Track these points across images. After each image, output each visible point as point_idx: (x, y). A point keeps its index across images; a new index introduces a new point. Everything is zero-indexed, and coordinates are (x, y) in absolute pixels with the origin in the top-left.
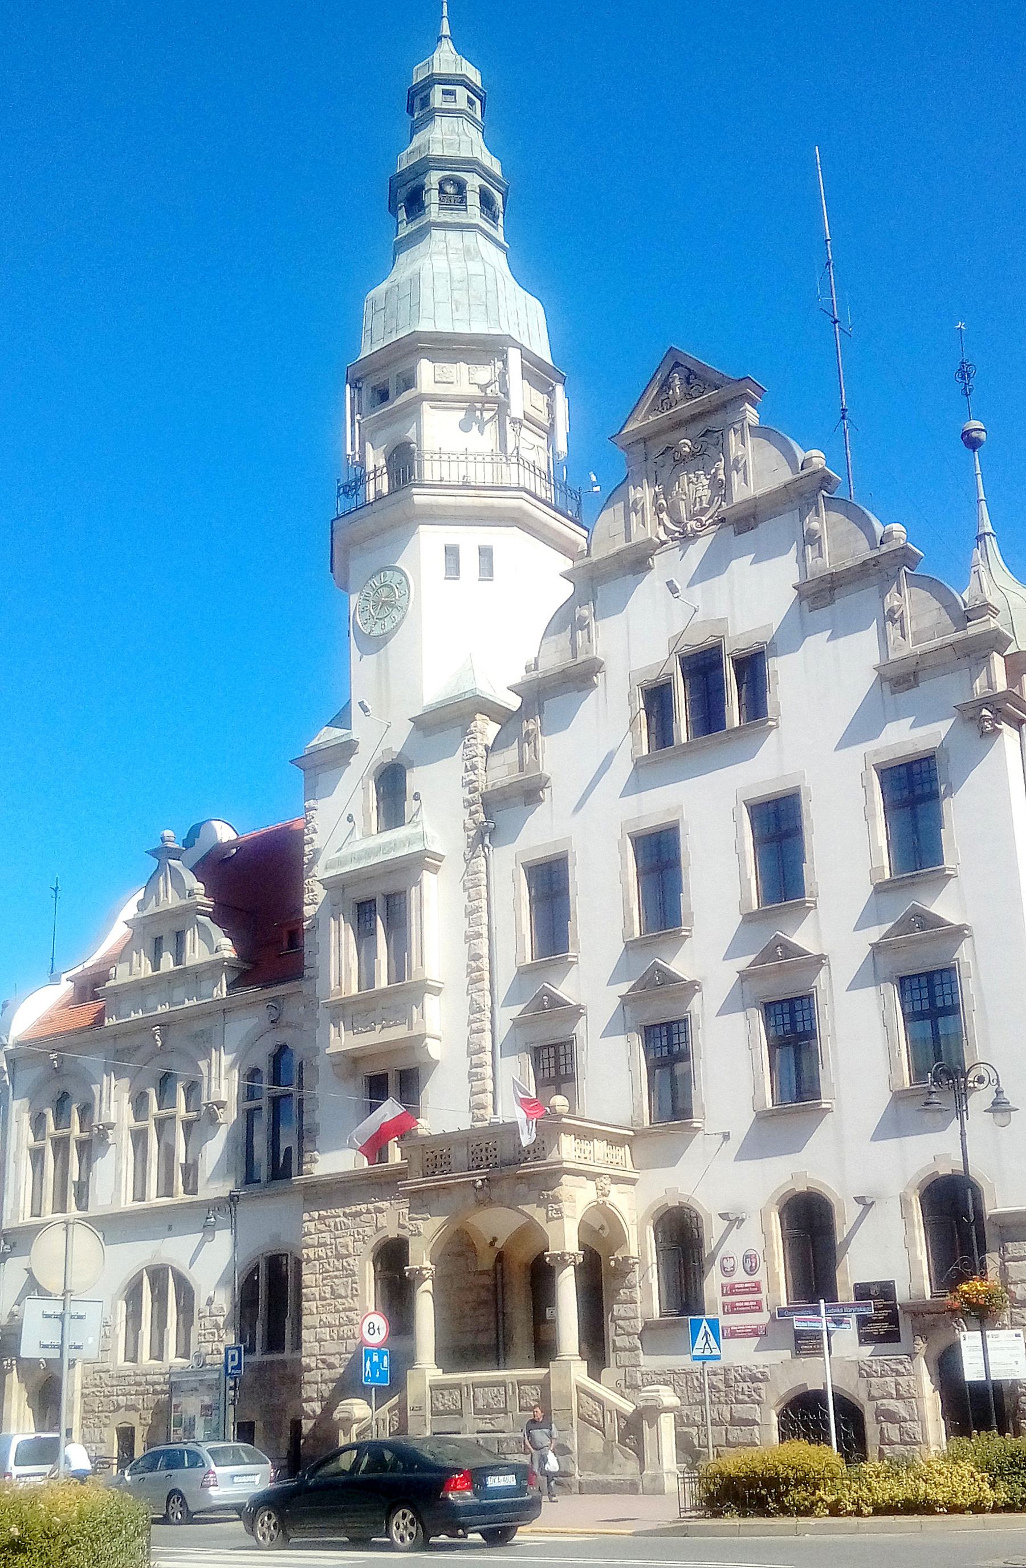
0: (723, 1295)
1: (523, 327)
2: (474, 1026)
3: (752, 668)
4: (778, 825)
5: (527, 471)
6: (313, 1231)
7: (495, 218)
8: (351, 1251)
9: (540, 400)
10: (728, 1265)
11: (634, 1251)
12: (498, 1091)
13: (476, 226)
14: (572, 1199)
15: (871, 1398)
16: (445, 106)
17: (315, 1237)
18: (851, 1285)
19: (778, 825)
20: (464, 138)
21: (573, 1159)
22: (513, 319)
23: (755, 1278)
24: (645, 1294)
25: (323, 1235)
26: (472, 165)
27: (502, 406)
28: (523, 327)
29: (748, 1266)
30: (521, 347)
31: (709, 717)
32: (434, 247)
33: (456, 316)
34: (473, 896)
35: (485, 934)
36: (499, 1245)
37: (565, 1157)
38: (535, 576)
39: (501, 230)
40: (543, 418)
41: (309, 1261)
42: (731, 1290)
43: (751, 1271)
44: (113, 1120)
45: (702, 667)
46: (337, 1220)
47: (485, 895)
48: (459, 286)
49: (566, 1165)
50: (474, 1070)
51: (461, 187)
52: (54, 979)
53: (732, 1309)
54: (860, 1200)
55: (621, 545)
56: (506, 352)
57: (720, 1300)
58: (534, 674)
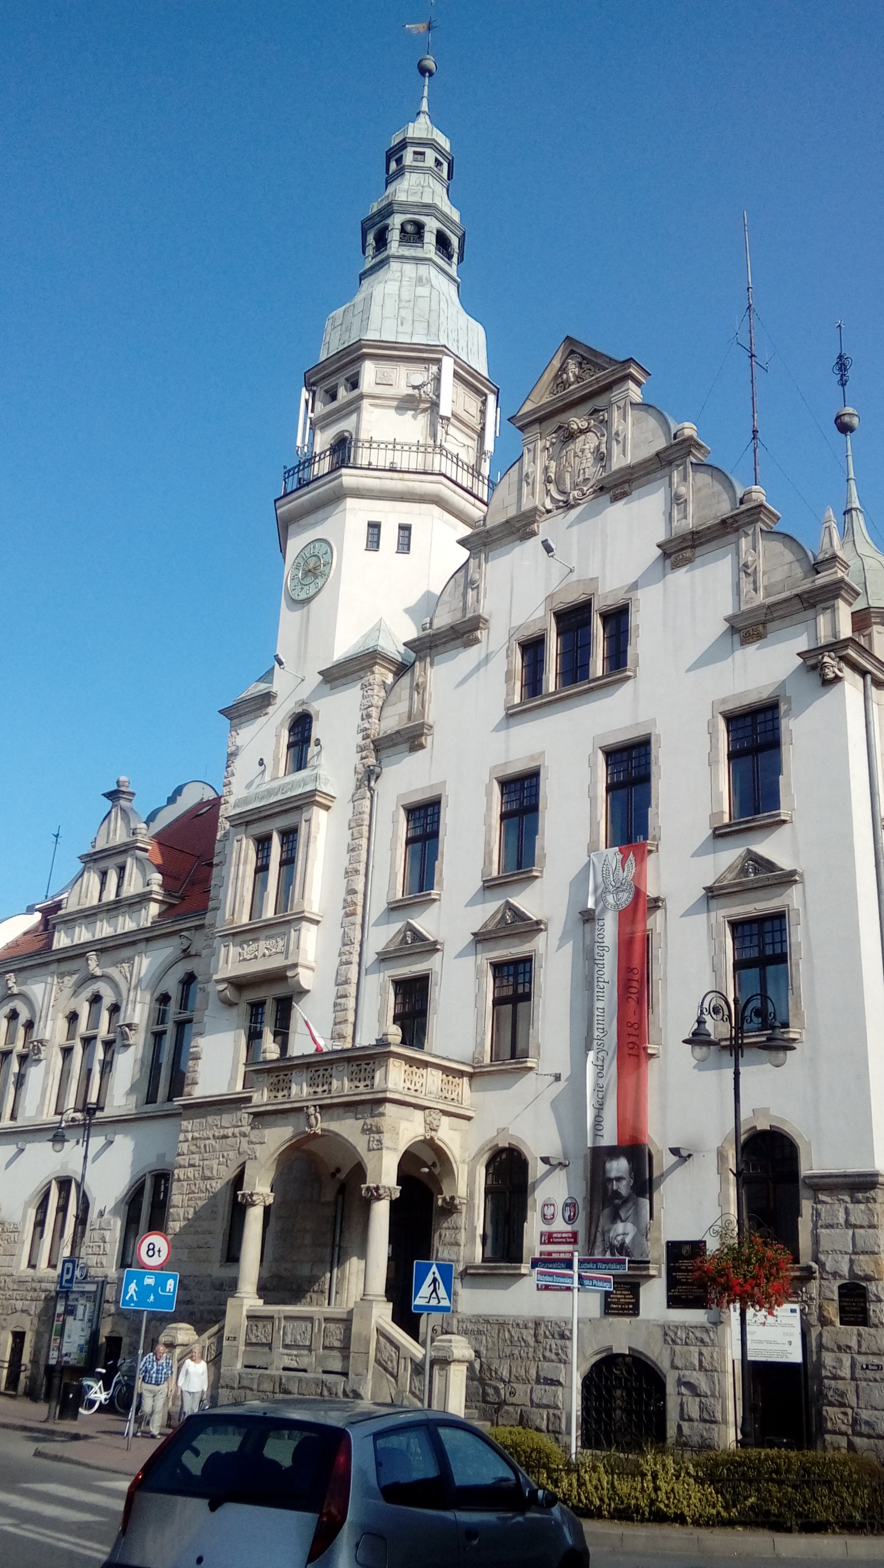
0: (541, 1243)
1: (462, 343)
2: (344, 958)
3: (618, 619)
4: (630, 768)
5: (449, 462)
6: (186, 1152)
7: (450, 257)
8: (215, 1173)
9: (472, 404)
10: (549, 1211)
11: (462, 1190)
12: (359, 1022)
14: (395, 1131)
15: (674, 1367)
17: (186, 1158)
18: (664, 1243)
19: (630, 768)
21: (401, 1089)
22: (453, 335)
24: (466, 1235)
25: (194, 1156)
26: (430, 209)
27: (435, 405)
28: (462, 343)
29: (567, 1215)
30: (456, 358)
31: (575, 669)
32: (390, 275)
33: (400, 329)
34: (356, 835)
35: (363, 871)
36: (342, 1176)
37: (390, 1085)
38: (441, 546)
39: (454, 267)
40: (475, 422)
41: (179, 1180)
42: (549, 1238)
44: (47, 1036)
45: (573, 619)
46: (207, 1142)
47: (366, 834)
48: (406, 305)
49: (389, 1095)
50: (339, 1001)
52: (30, 910)
54: (675, 1151)
55: (512, 512)
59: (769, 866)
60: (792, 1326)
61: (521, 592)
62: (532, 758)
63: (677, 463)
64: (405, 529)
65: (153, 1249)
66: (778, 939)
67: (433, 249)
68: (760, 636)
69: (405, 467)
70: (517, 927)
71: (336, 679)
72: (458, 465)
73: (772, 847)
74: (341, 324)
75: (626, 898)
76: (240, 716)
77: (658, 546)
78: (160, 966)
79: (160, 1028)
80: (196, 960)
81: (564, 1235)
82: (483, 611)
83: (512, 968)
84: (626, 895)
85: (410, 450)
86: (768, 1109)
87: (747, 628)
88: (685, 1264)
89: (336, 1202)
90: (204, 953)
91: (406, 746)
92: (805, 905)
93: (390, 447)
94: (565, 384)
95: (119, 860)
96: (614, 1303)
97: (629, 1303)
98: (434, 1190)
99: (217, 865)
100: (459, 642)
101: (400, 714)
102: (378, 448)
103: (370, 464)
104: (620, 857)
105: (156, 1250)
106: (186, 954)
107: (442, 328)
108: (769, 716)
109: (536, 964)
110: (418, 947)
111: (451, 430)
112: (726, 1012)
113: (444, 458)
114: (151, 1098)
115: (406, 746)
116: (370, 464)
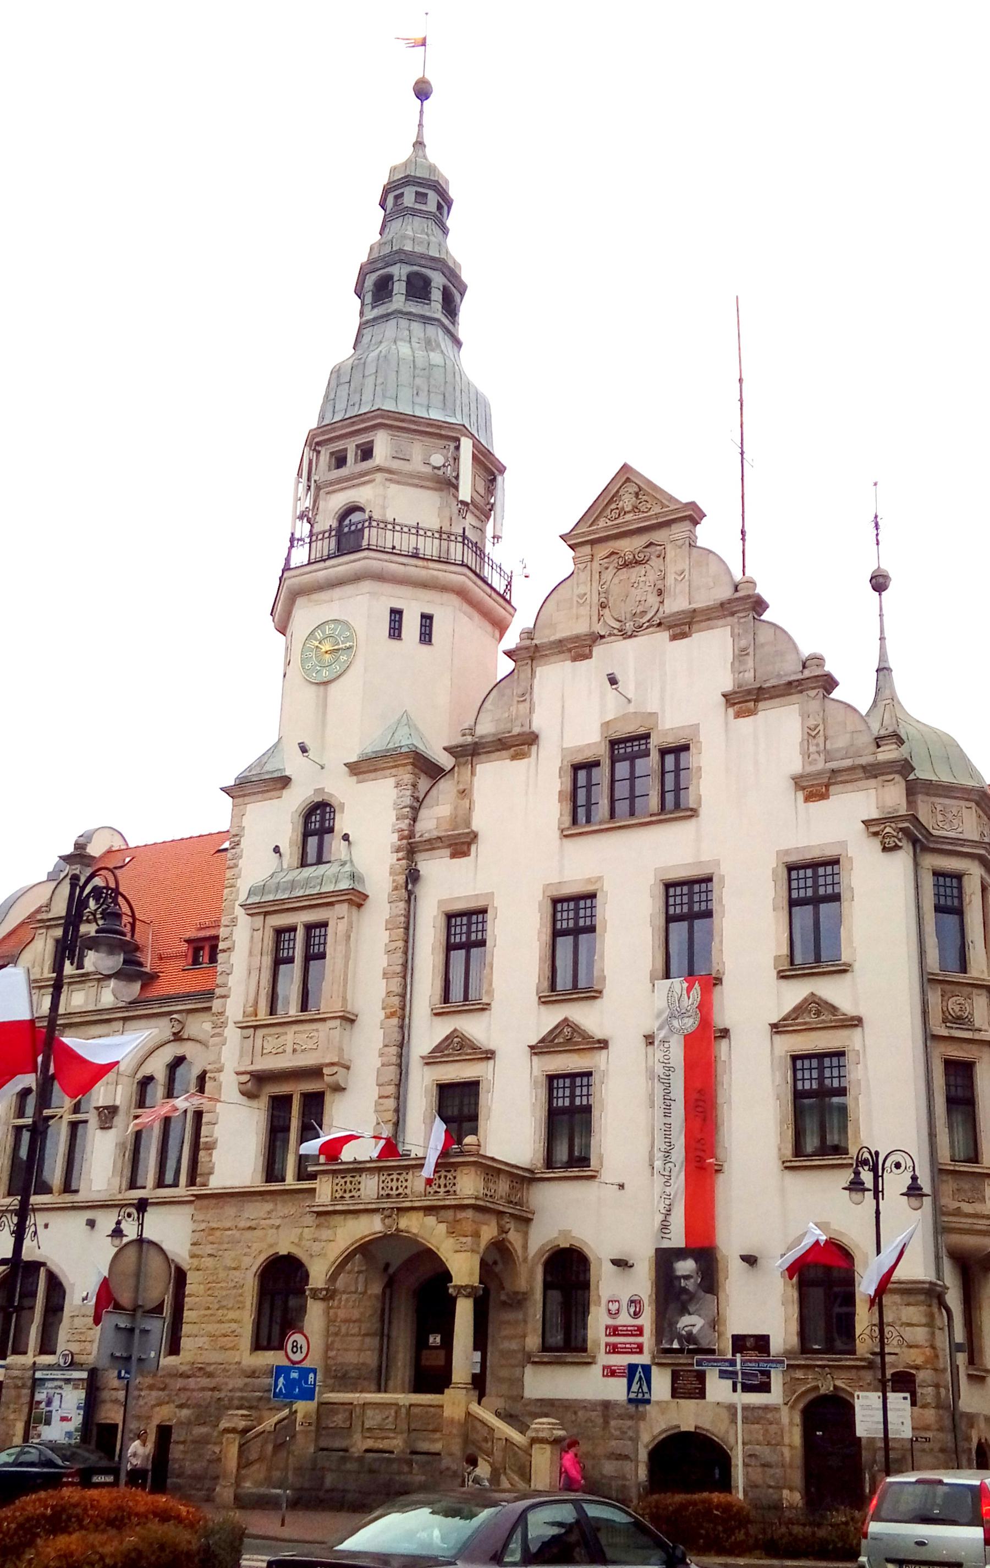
10: (614, 1307)
16: (418, 206)
20: (432, 238)
23: (638, 1322)
29: (632, 1310)
30: (472, 436)
33: (417, 400)
36: (391, 1271)
42: (614, 1331)
43: (636, 1315)
51: (427, 282)
53: (614, 1349)
56: (458, 440)
57: (604, 1340)
58: (469, 739)
59: (833, 1009)
60: (904, 1410)
61: (574, 711)
62: (589, 881)
63: (742, 615)
64: (427, 619)
67: (439, 307)
68: (824, 796)
70: (577, 1043)
75: (690, 1024)
76: (244, 796)
77: (724, 696)
82: (535, 727)
83: (568, 1081)
84: (691, 1020)
87: (814, 788)
89: (384, 1293)
91: (447, 852)
93: (414, 531)
97: (696, 1388)
99: (224, 951)
101: (438, 818)
103: (394, 548)
104: (685, 985)
106: (177, 1037)
107: (458, 402)
109: (595, 1079)
110: (467, 1054)
115: (447, 852)
116: (394, 548)
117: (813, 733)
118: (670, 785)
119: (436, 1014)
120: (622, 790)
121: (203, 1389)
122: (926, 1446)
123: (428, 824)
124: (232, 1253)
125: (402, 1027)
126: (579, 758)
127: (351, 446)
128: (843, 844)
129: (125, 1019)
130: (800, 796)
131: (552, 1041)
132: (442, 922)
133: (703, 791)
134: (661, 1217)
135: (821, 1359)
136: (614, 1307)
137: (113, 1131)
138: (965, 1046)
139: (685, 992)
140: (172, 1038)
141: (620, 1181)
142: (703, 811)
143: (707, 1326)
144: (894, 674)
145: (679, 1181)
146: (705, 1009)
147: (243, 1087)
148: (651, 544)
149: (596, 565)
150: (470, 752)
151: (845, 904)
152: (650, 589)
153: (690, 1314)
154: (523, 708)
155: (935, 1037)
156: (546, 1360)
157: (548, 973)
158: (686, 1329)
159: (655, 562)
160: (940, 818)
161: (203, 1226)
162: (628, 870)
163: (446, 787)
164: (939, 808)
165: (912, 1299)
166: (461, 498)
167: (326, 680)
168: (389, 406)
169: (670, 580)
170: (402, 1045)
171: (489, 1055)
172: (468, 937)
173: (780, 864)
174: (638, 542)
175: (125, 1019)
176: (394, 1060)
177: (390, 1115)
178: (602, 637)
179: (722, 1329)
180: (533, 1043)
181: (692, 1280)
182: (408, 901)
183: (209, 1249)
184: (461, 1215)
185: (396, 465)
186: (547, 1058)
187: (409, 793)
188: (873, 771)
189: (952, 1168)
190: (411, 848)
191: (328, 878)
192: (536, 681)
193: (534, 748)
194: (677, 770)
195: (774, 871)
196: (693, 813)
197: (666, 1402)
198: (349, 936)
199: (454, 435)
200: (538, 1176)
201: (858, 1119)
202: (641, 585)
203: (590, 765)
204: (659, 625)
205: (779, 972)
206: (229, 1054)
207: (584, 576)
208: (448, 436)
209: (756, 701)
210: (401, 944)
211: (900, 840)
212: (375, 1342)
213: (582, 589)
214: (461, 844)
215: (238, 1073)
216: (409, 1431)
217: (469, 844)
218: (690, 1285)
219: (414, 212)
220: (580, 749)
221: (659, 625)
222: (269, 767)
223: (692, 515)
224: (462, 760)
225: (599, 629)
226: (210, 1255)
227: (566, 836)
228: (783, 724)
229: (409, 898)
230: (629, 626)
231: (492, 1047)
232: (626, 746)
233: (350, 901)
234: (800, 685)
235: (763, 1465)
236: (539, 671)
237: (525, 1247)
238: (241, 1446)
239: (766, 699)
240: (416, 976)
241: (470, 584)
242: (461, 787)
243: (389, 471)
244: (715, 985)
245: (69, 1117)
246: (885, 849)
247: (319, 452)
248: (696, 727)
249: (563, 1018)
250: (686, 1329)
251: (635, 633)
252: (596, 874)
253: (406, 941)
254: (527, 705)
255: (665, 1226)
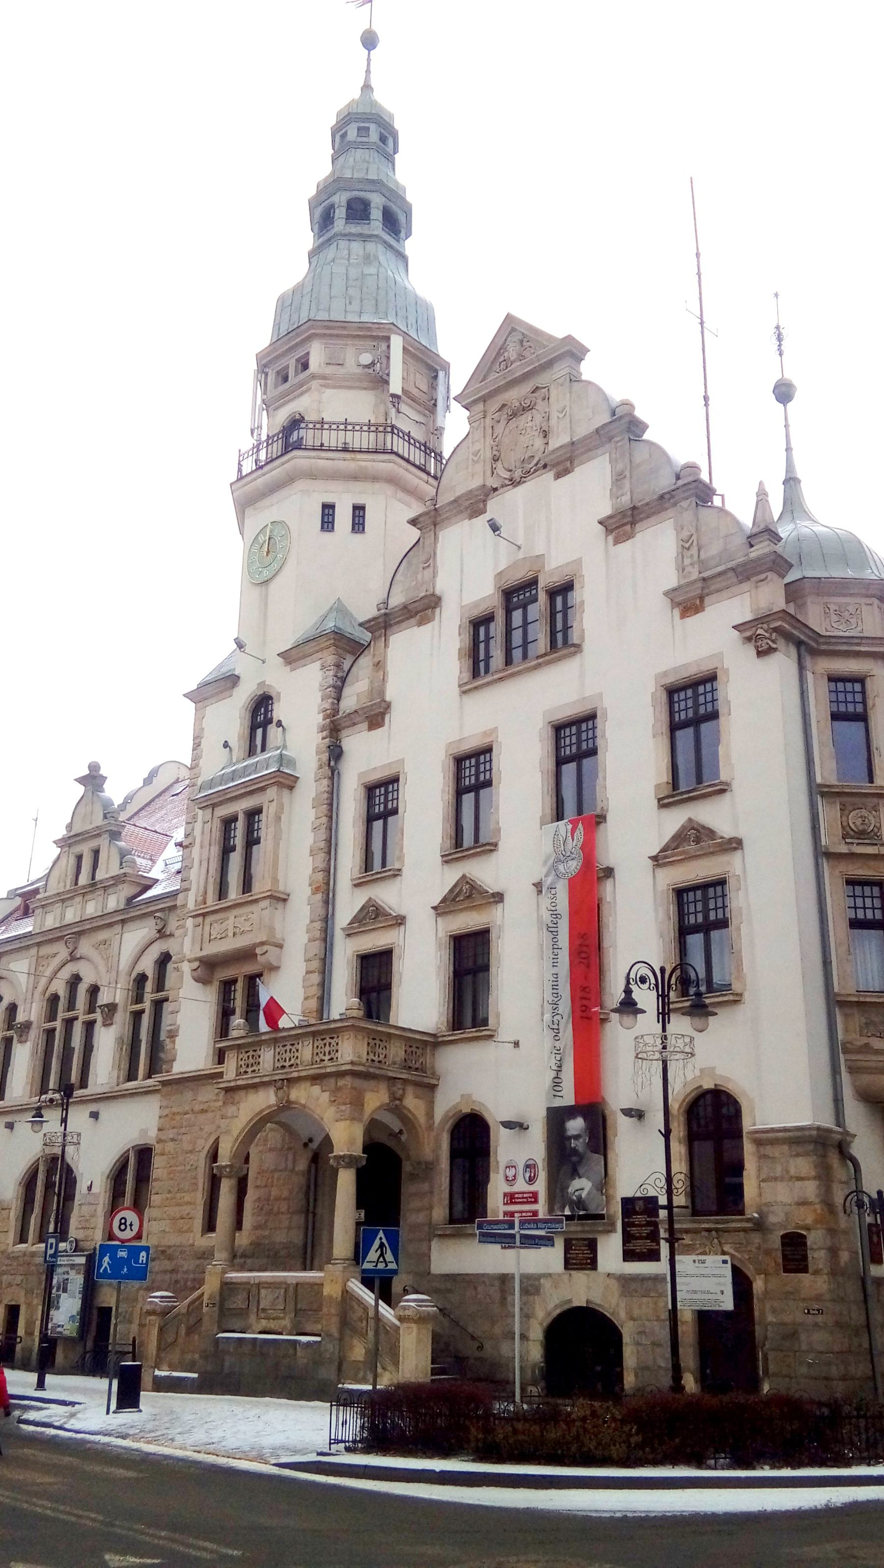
0: (504, 1204)
13: (377, 236)
23: (532, 1188)
28: (412, 320)
29: (527, 1175)
33: (349, 308)
36: (314, 1145)
42: (511, 1198)
43: (531, 1180)
56: (388, 339)
62: (485, 734)
64: (359, 511)
65: (125, 1224)
66: (720, 904)
69: (357, 445)
71: (295, 661)
72: (410, 443)
73: (712, 814)
74: (291, 305)
75: (574, 866)
77: (600, 523)
78: (137, 945)
79: (138, 1007)
80: (171, 940)
81: (525, 1195)
85: (361, 430)
86: (713, 1068)
88: (640, 1219)
89: (309, 1171)
90: (177, 933)
91: (365, 725)
92: (745, 871)
94: (508, 362)
95: (93, 844)
96: (573, 1259)
97: (589, 1258)
98: (403, 1156)
100: (413, 621)
102: (330, 429)
103: (322, 445)
105: (128, 1223)
106: (162, 934)
108: (708, 687)
109: (493, 935)
110: (381, 922)
111: (403, 408)
112: (653, 981)
113: (395, 437)
114: (131, 1076)
116: (322, 445)
117: (687, 545)
118: (559, 626)
119: (356, 886)
120: (517, 637)
121: (165, 1272)
122: (820, 1319)
123: (350, 701)
124: (188, 1137)
125: (326, 902)
126: (476, 613)
127: (291, 362)
128: (720, 656)
129: (123, 922)
130: (677, 612)
131: (454, 900)
132: (361, 794)
133: (586, 626)
134: (554, 1074)
135: (708, 1222)
136: (511, 1173)
137: (114, 1026)
138: (872, 863)
139: (569, 834)
140: (158, 935)
141: (512, 1039)
142: (587, 646)
143: (594, 1191)
144: (802, 484)
145: (567, 1034)
146: (588, 850)
147: (195, 974)
148: (537, 388)
149: (488, 420)
150: (384, 624)
151: (722, 719)
152: (536, 433)
153: (580, 1177)
154: (428, 573)
155: (830, 855)
156: (448, 1232)
157: (451, 831)
158: (576, 1193)
159: (541, 405)
160: (834, 618)
161: (166, 1112)
162: (518, 717)
163: (365, 662)
164: (833, 607)
165: (800, 1149)
166: (391, 391)
167: (266, 579)
168: (322, 316)
169: (553, 421)
170: (327, 920)
171: (400, 921)
172: (386, 806)
173: (659, 688)
174: (524, 389)
175: (123, 922)
176: (318, 934)
177: (315, 991)
178: (495, 490)
179: (611, 1192)
180: (435, 904)
181: (581, 1140)
182: (332, 778)
183: (171, 1134)
184: (341, 1083)
185: (329, 370)
186: (450, 918)
187: (331, 673)
188: (746, 573)
189: (856, 999)
190: (335, 729)
191: (264, 764)
192: (439, 545)
193: (438, 610)
194: (566, 608)
195: (653, 695)
196: (578, 648)
197: (559, 1275)
198: (280, 818)
199: (384, 334)
200: (440, 1039)
201: (740, 951)
202: (528, 430)
203: (486, 620)
204: (545, 466)
205: (659, 800)
206: (188, 944)
207: (478, 434)
208: (377, 336)
209: (633, 523)
210: (324, 820)
211: (774, 641)
212: (299, 1220)
213: (478, 446)
214: (376, 716)
215: (189, 961)
216: (297, 1311)
217: (383, 715)
218: (579, 1145)
219: (355, 145)
220: (476, 604)
221: (545, 466)
222: (224, 670)
223: (573, 351)
224: (377, 634)
225: (492, 482)
226: (172, 1140)
227: (464, 692)
228: (659, 541)
229: (333, 774)
230: (517, 474)
231: (402, 913)
232: (516, 594)
233: (280, 785)
234: (673, 497)
235: (654, 1344)
236: (441, 535)
237: (430, 1114)
238: (161, 1330)
239: (641, 520)
240: (340, 851)
241: (401, 472)
242: (376, 660)
243: (324, 378)
244: (598, 823)
245: (82, 1018)
246: (760, 654)
247: (266, 375)
248: (579, 562)
249: (460, 875)
250: (576, 1193)
251: (523, 479)
252: (491, 726)
253: (331, 817)
254: (431, 569)
255: (557, 1083)
